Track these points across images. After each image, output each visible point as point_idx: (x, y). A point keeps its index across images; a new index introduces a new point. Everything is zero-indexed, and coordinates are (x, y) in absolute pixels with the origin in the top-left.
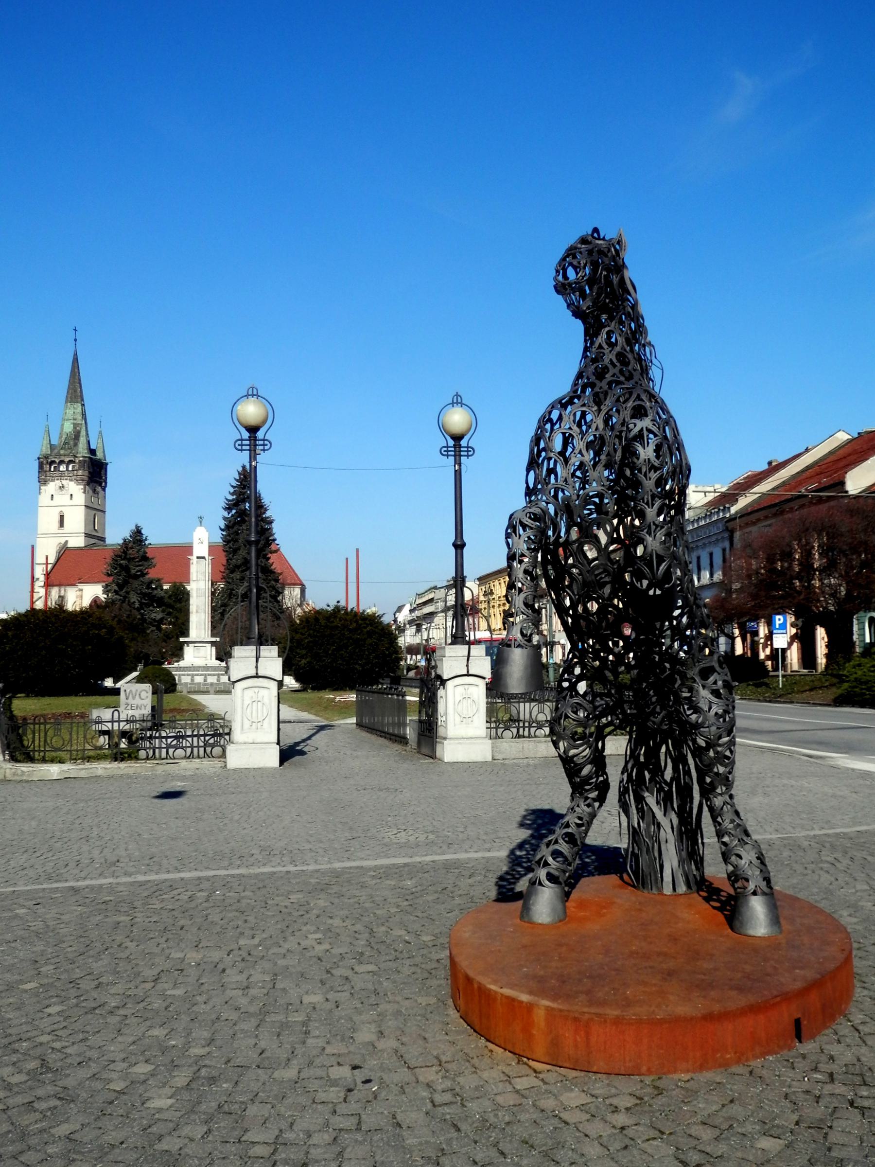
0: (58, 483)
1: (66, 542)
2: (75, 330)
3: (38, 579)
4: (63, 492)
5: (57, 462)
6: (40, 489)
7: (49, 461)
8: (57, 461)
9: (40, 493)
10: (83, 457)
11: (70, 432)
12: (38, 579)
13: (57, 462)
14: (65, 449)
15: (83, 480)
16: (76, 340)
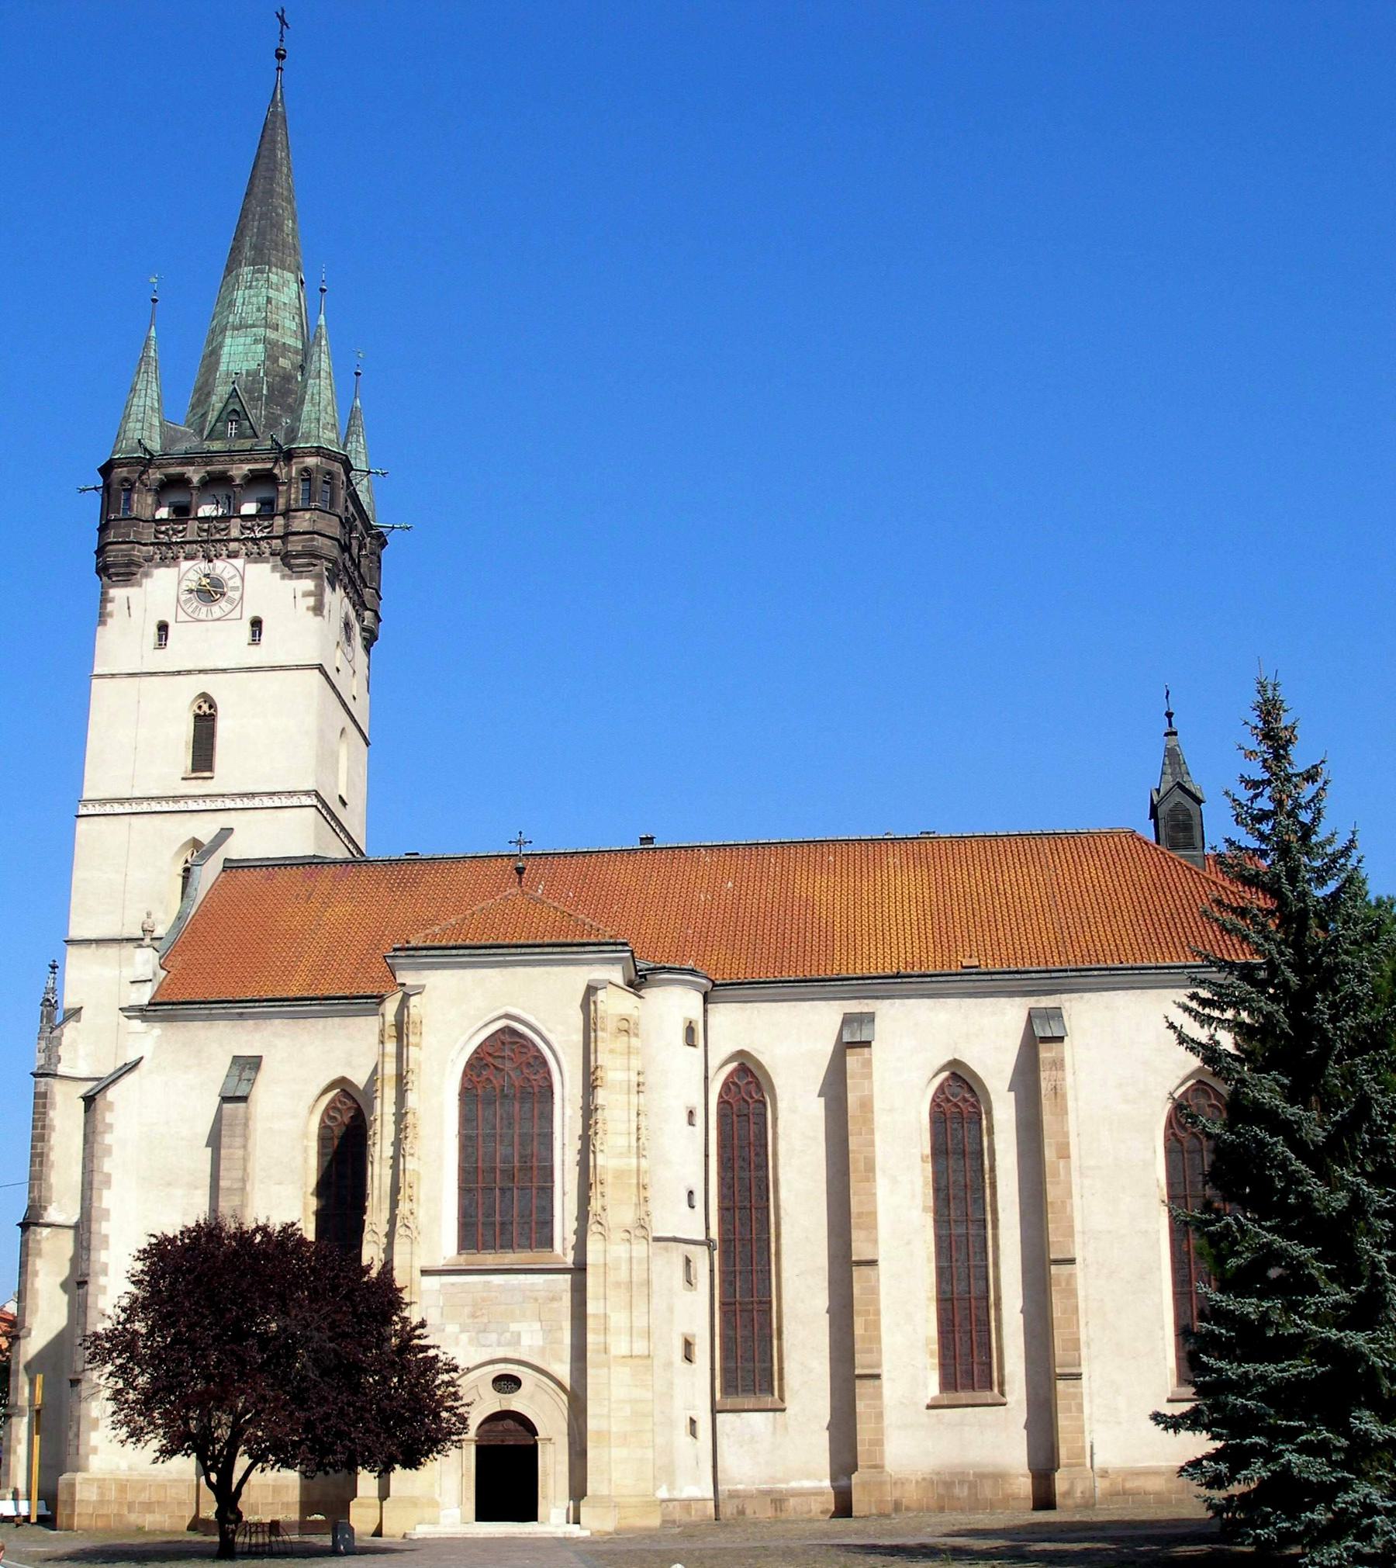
0: (192, 571)
1: (226, 833)
2: (283, 22)
3: (75, 1013)
4: (216, 610)
5: (196, 479)
6: (104, 599)
7: (155, 475)
8: (195, 474)
9: (102, 618)
10: (319, 451)
11: (253, 374)
12: (75, 1013)
13: (196, 479)
14: (222, 436)
15: (313, 555)
16: (280, 56)
